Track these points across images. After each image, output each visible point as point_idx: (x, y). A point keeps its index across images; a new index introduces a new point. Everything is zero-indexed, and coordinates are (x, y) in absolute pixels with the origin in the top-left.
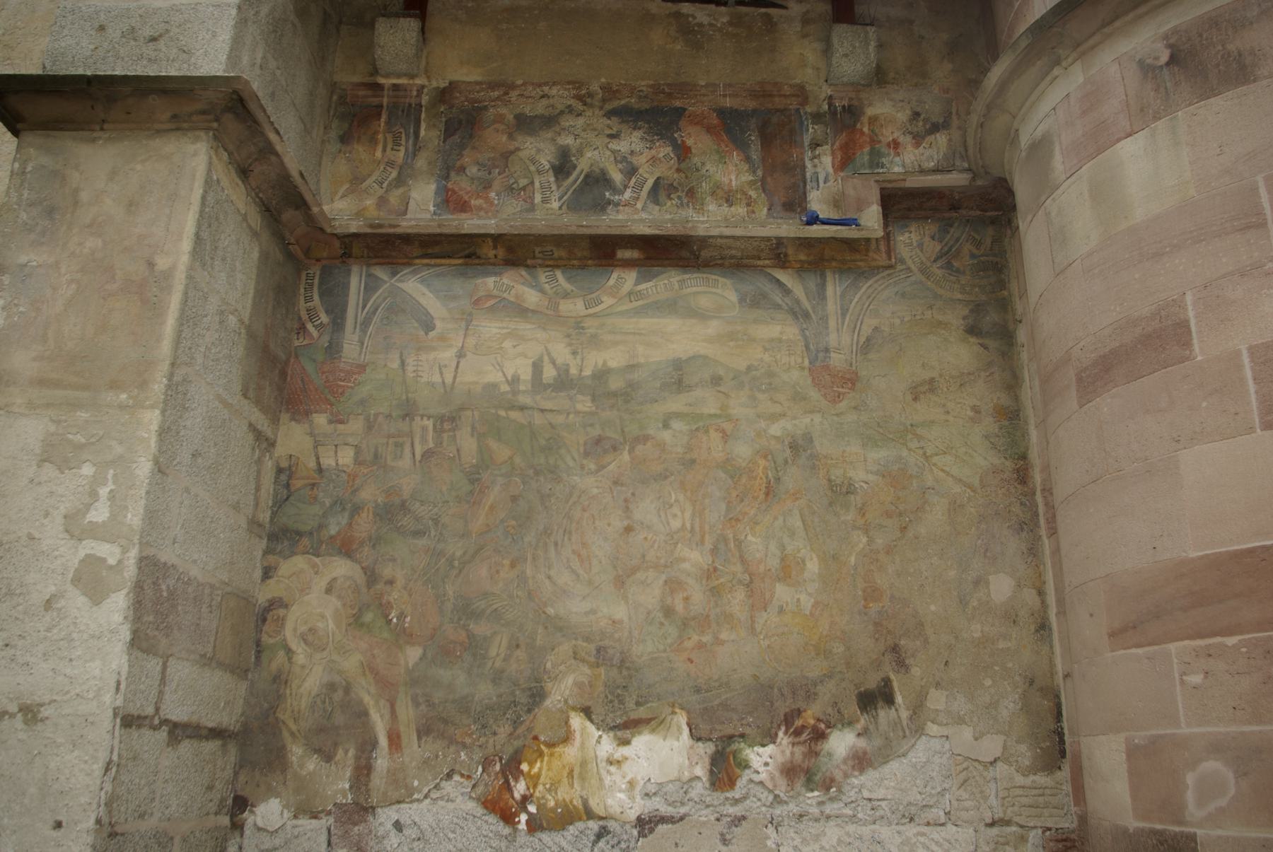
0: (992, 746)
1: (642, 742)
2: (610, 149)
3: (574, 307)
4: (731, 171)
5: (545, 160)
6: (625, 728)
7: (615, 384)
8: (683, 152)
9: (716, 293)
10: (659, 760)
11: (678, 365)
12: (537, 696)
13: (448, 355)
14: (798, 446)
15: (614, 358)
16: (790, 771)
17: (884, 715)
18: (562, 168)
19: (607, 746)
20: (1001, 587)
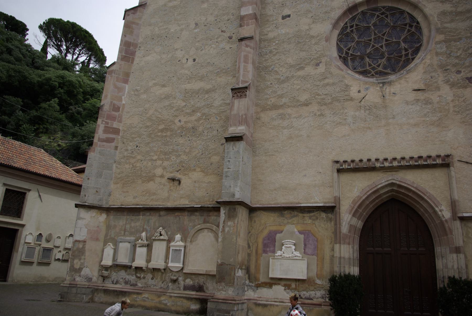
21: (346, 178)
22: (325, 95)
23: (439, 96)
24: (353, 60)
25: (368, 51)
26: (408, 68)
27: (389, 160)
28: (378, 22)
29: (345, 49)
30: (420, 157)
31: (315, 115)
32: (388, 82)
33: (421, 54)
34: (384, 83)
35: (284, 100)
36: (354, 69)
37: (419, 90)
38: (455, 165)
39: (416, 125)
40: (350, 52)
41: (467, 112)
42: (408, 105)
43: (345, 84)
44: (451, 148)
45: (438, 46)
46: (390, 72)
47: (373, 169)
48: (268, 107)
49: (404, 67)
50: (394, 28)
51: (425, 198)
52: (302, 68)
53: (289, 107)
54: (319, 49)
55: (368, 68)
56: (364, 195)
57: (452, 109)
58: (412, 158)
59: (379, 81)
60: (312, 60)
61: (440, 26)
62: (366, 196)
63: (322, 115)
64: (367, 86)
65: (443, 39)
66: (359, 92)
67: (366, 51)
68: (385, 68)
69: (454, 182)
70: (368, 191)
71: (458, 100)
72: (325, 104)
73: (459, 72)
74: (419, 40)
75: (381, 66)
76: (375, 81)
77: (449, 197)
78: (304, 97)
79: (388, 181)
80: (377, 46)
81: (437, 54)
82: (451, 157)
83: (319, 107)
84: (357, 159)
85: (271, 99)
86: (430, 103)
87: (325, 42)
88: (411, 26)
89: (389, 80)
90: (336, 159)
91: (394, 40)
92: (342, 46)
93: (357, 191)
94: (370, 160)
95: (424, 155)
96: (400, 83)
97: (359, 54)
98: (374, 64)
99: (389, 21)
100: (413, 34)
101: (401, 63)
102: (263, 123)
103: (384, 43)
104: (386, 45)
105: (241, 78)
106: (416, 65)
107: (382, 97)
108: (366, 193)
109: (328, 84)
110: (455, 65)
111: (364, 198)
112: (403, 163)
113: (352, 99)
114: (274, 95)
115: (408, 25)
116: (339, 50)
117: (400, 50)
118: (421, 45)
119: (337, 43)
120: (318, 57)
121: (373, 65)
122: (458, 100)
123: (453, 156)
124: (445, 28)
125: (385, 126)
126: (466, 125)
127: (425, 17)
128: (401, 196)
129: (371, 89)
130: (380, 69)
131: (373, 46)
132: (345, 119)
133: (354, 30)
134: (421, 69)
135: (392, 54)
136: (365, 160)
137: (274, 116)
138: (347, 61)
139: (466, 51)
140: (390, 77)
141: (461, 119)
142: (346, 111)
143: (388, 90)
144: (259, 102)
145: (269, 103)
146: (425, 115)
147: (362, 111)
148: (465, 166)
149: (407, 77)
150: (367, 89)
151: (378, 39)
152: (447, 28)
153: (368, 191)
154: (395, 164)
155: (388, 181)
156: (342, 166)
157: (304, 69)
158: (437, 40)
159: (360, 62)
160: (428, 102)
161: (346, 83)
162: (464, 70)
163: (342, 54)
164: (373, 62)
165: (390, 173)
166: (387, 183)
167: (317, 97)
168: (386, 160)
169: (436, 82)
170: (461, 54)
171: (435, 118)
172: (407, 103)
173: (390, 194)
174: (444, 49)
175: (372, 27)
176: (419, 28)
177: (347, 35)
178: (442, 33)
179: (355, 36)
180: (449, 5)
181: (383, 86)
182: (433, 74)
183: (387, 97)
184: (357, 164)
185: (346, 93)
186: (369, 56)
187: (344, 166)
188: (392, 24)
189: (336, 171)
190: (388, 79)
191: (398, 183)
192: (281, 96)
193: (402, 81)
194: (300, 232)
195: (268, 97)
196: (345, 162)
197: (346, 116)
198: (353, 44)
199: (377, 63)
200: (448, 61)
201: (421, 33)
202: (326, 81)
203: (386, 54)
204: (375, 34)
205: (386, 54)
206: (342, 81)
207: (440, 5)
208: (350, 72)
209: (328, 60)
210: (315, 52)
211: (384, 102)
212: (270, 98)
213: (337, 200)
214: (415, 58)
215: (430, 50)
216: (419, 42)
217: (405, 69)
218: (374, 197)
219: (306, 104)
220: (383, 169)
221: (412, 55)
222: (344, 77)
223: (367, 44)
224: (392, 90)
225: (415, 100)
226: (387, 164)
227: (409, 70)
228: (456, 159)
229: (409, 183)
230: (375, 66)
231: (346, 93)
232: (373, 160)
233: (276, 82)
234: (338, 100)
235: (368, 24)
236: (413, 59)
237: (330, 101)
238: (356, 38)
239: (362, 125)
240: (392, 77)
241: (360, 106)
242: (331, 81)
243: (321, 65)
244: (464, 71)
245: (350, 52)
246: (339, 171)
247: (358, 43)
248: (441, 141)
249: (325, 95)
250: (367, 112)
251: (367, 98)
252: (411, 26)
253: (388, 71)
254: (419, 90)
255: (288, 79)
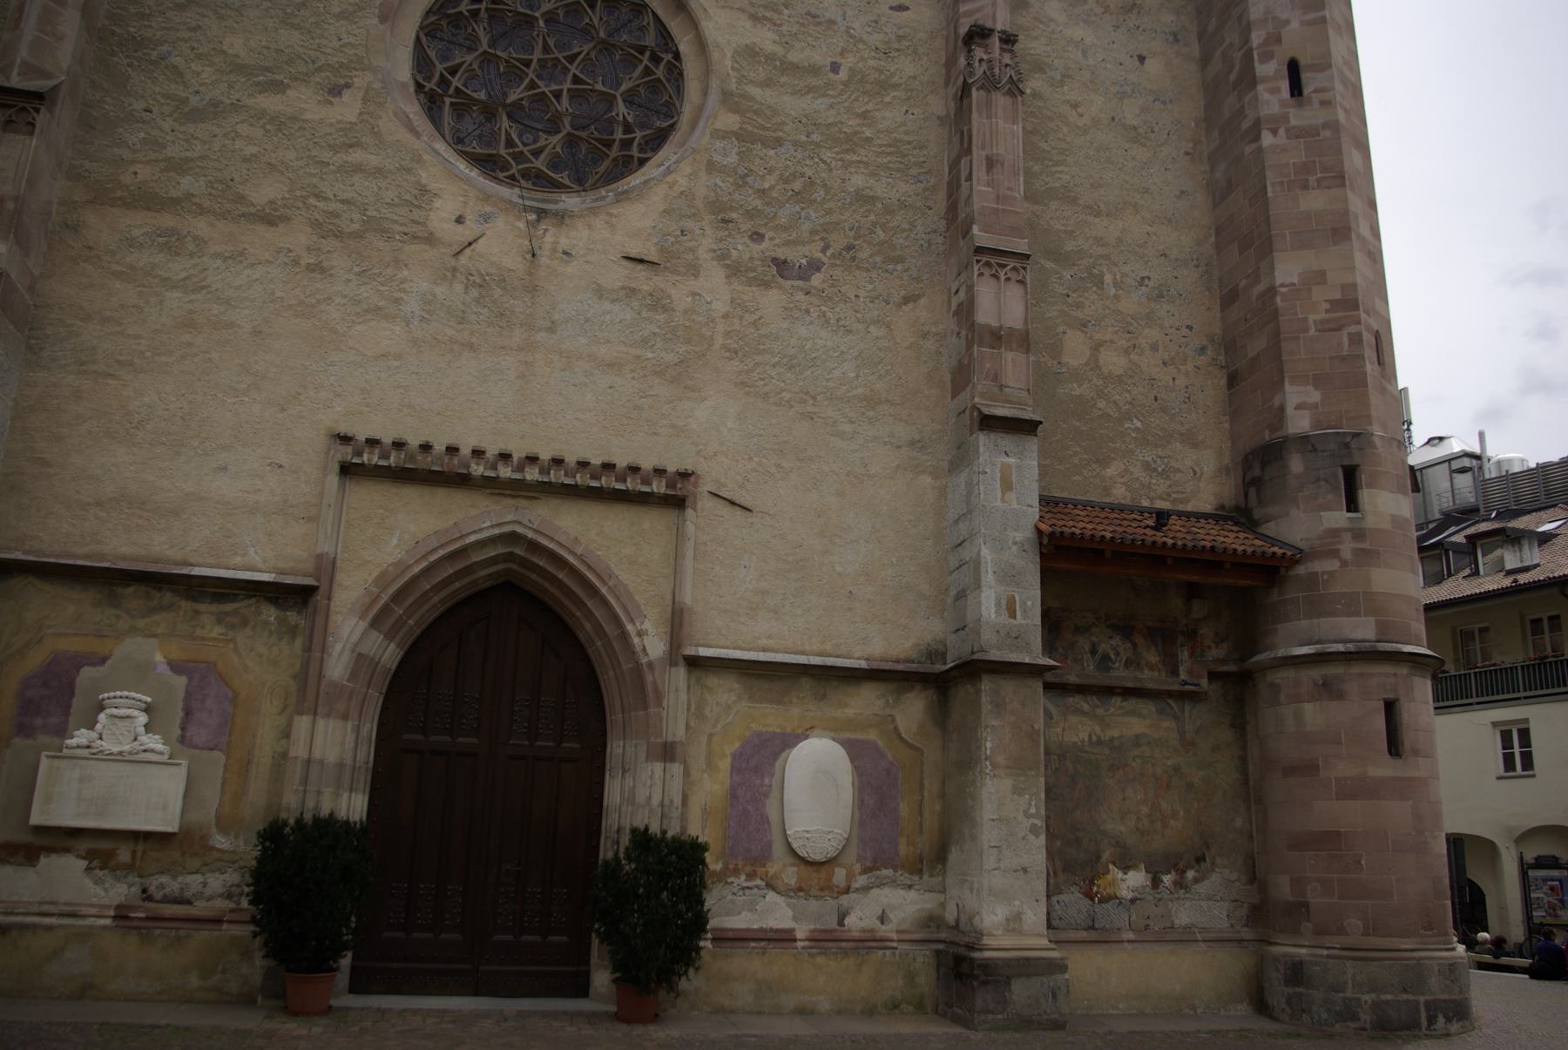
0: (1234, 876)
1: (1131, 873)
2: (1112, 644)
3: (1100, 711)
4: (1152, 657)
5: (1087, 648)
6: (1125, 869)
7: (1116, 743)
8: (1135, 646)
9: (1147, 707)
10: (1136, 879)
11: (1137, 736)
12: (1099, 857)
13: (1059, 730)
14: (1177, 769)
15: (1115, 733)
16: (1175, 883)
17: (1203, 865)
18: (1093, 652)
19: (1120, 875)
20: (1239, 822)
21: (368, 497)
22: (343, 202)
23: (694, 294)
24: (460, 110)
25: (512, 98)
26: (622, 185)
27: (515, 459)
28: (561, 12)
29: (440, 67)
30: (608, 467)
31: (296, 263)
32: (556, 214)
33: (667, 154)
34: (541, 213)
35: (186, 182)
36: (458, 142)
37: (641, 261)
38: (699, 506)
39: (613, 366)
40: (456, 82)
41: (759, 358)
42: (600, 297)
43: (418, 182)
44: (698, 452)
45: (719, 144)
46: (567, 182)
47: (460, 481)
48: (118, 194)
49: (612, 177)
50: (607, 47)
51: (604, 590)
52: (278, 87)
53: (202, 211)
54: (352, 39)
55: (502, 152)
56: (417, 561)
57: (719, 341)
58: (583, 464)
59: (527, 203)
60: (319, 70)
61: (733, 86)
62: (424, 564)
63: (317, 268)
64: (488, 209)
65: (736, 127)
66: (460, 220)
67: (505, 95)
68: (555, 165)
69: (690, 554)
70: (434, 550)
71: (741, 318)
72: (339, 235)
73: (757, 237)
74: (670, 110)
75: (543, 156)
76: (516, 199)
77: (669, 597)
78: (264, 192)
79: (499, 525)
80: (543, 87)
81: (711, 167)
82: (692, 479)
83: (314, 238)
84: (414, 441)
85: (137, 168)
86: (665, 309)
87: (375, 21)
88: (656, 59)
89: (561, 206)
90: (343, 429)
91: (599, 87)
92: (432, 55)
93: (397, 546)
94: (457, 450)
95: (621, 462)
96: (590, 226)
97: (482, 95)
98: (525, 145)
99: (596, 22)
100: (655, 86)
101: (606, 163)
102: (90, 248)
103: (567, 85)
104: (573, 95)
105: (23, 53)
106: (646, 182)
107: (529, 256)
108: (424, 557)
109: (358, 169)
110: (751, 214)
111: (417, 569)
112: (556, 476)
113: (430, 240)
114: (153, 156)
115: (648, 54)
116: (422, 62)
117: (611, 121)
118: (672, 126)
119: (418, 39)
120: (341, 65)
121: (521, 147)
122: (741, 318)
123: (698, 477)
124: (744, 96)
125: (520, 349)
126: (747, 393)
127: (701, 44)
128: (534, 576)
129: (500, 223)
130: (540, 164)
131: (532, 85)
132: (397, 301)
133: (483, 14)
134: (658, 197)
135: (583, 128)
136: (439, 448)
137: (136, 233)
138: (441, 108)
139: (786, 181)
140: (563, 197)
141: (740, 373)
142: (406, 273)
143: (551, 236)
144: (87, 164)
145: (127, 179)
146: (645, 341)
147: (459, 288)
148: (725, 510)
149: (614, 211)
150: (486, 218)
151: (550, 68)
152: (752, 99)
153: (434, 550)
154: (532, 474)
155: (499, 525)
156: (359, 454)
157: (283, 92)
158: (719, 125)
159: (481, 125)
160: (658, 303)
161: (423, 181)
162: (769, 234)
163: (428, 79)
164: (520, 136)
165: (510, 501)
166: (497, 531)
167: (312, 201)
168: (505, 457)
169: (692, 250)
170: (772, 188)
171: (670, 358)
172: (600, 292)
173: (500, 567)
174: (733, 159)
175: (541, 23)
176: (676, 73)
177: (457, 21)
178: (735, 109)
179: (481, 33)
180: (770, 35)
181: (538, 220)
182: (689, 224)
183: (543, 260)
184: (412, 458)
185: (416, 214)
186: (514, 112)
187: (365, 457)
188: (602, 35)
189: (336, 468)
190: (556, 202)
191: (530, 535)
192: (179, 167)
193: (598, 222)
194: (176, 667)
195: (127, 155)
196: (372, 442)
197: (404, 291)
198: (469, 58)
199: (535, 142)
200: (736, 196)
201: (680, 90)
202: (356, 156)
203: (567, 121)
204: (546, 49)
205: (567, 121)
206: (409, 171)
207: (748, 24)
208: (441, 146)
209: (377, 85)
210: (336, 44)
211: (531, 274)
212: (134, 162)
213: (327, 567)
214: (647, 159)
215: (694, 151)
216: (669, 116)
217: (614, 186)
218: (451, 571)
219: (270, 218)
220: (492, 485)
221: (642, 150)
222: (419, 160)
223: (514, 73)
224: (564, 243)
225: (623, 288)
226: (505, 472)
227: (625, 192)
228: (706, 486)
229: (562, 539)
230: (525, 150)
231: (416, 214)
232: (466, 451)
233: (167, 110)
234: (384, 231)
235: (531, 7)
236: (642, 162)
237: (355, 227)
238: (485, 40)
239: (450, 332)
240: (570, 202)
241: (455, 269)
242: (372, 160)
243: (347, 95)
244: (771, 239)
245: (456, 82)
246: (346, 470)
247: (487, 59)
248: (673, 426)
249: (343, 202)
250: (474, 293)
251: (480, 246)
252: (656, 59)
253: (563, 177)
254: (641, 261)
255: (215, 110)
